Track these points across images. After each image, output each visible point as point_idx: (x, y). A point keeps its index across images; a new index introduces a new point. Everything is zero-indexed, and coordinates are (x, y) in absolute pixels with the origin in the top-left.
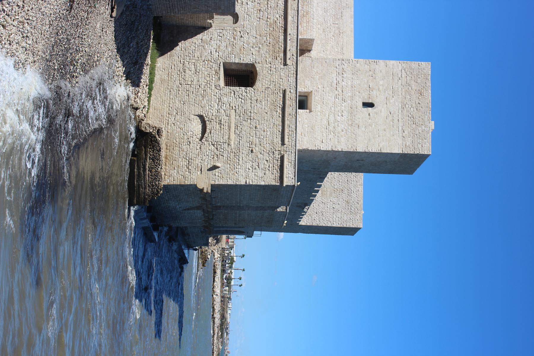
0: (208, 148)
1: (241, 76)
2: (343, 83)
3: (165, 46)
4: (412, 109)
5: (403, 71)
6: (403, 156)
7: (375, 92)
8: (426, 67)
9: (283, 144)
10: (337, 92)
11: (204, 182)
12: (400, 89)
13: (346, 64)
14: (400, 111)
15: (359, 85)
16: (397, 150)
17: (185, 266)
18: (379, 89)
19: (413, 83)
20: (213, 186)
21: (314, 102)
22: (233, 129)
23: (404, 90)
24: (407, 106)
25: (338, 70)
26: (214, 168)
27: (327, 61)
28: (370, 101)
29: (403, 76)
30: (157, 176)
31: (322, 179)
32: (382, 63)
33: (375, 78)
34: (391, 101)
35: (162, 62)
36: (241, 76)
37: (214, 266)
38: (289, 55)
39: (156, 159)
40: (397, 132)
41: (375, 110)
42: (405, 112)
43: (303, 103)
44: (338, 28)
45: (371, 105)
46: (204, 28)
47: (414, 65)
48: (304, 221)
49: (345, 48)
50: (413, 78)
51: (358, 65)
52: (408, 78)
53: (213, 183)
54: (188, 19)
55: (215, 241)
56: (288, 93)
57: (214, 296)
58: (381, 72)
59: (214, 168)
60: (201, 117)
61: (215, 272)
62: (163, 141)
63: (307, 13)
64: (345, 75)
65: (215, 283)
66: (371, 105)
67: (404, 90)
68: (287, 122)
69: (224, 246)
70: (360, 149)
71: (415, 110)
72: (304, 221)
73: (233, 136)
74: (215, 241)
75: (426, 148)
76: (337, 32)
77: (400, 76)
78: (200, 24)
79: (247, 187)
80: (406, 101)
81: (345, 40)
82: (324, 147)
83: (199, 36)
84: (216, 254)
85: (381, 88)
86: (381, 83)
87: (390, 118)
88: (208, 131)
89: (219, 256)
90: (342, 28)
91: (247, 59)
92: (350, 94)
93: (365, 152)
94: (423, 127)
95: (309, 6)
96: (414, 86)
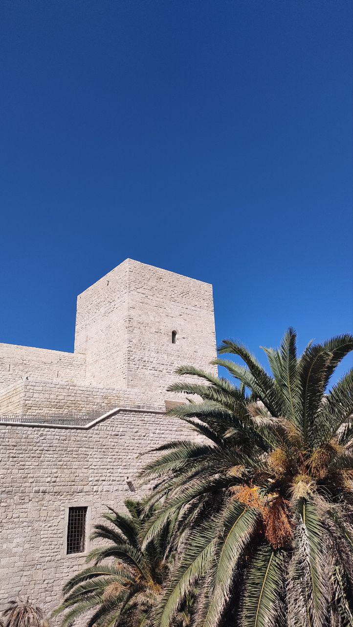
2: (154, 362)
4: (176, 292)
5: (138, 290)
7: (162, 327)
10: (164, 371)
12: (157, 299)
13: (134, 355)
14: (179, 304)
15: (155, 344)
18: (158, 322)
19: (149, 283)
23: (158, 295)
24: (173, 296)
25: (140, 367)
27: (130, 378)
28: (171, 334)
29: (143, 292)
33: (148, 324)
34: (169, 311)
40: (197, 312)
41: (179, 331)
42: (179, 299)
44: (15, 365)
45: (174, 334)
49: (45, 361)
50: (145, 282)
51: (133, 340)
52: (145, 287)
58: (140, 316)
63: (106, 398)
64: (146, 359)
66: (174, 334)
67: (158, 295)
71: (176, 289)
76: (21, 367)
77: (144, 296)
80: (168, 296)
81: (35, 358)
85: (157, 320)
86: (152, 318)
87: (185, 316)
90: (17, 361)
92: (166, 357)
94: (190, 285)
95: (94, 394)
96: (152, 283)
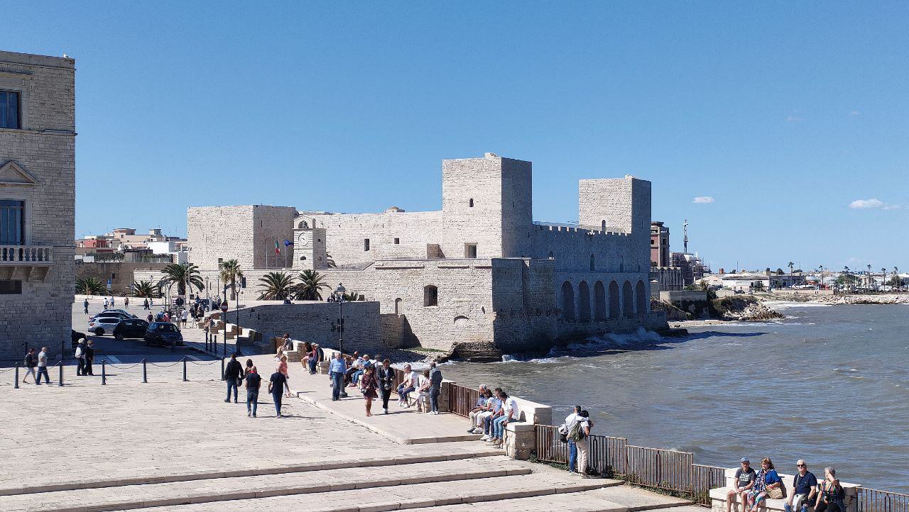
0: (472, 315)
1: (432, 295)
3: (416, 343)
6: (504, 176)
8: (445, 162)
9: (468, 267)
11: (491, 317)
16: (500, 182)
17: (689, 332)
19: (456, 173)
20: (494, 311)
21: (471, 241)
22: (461, 299)
26: (483, 309)
30: (482, 345)
31: (542, 228)
32: (444, 195)
35: (424, 344)
36: (432, 295)
37: (857, 303)
38: (419, 266)
39: (470, 345)
43: (472, 251)
45: (472, 200)
46: (405, 320)
47: (445, 171)
48: (628, 230)
53: (492, 311)
54: (400, 329)
55: (751, 304)
56: (439, 266)
57: (897, 302)
59: (483, 309)
60: (455, 319)
61: (865, 302)
62: (461, 340)
65: (881, 301)
66: (472, 200)
68: (456, 265)
69: (832, 292)
70: (500, 208)
72: (628, 230)
73: (465, 299)
74: (751, 304)
75: (499, 162)
78: (402, 322)
79: (494, 289)
82: (500, 234)
83: (410, 322)
84: (840, 302)
88: (463, 315)
89: (843, 298)
91: (422, 291)
93: (502, 203)
